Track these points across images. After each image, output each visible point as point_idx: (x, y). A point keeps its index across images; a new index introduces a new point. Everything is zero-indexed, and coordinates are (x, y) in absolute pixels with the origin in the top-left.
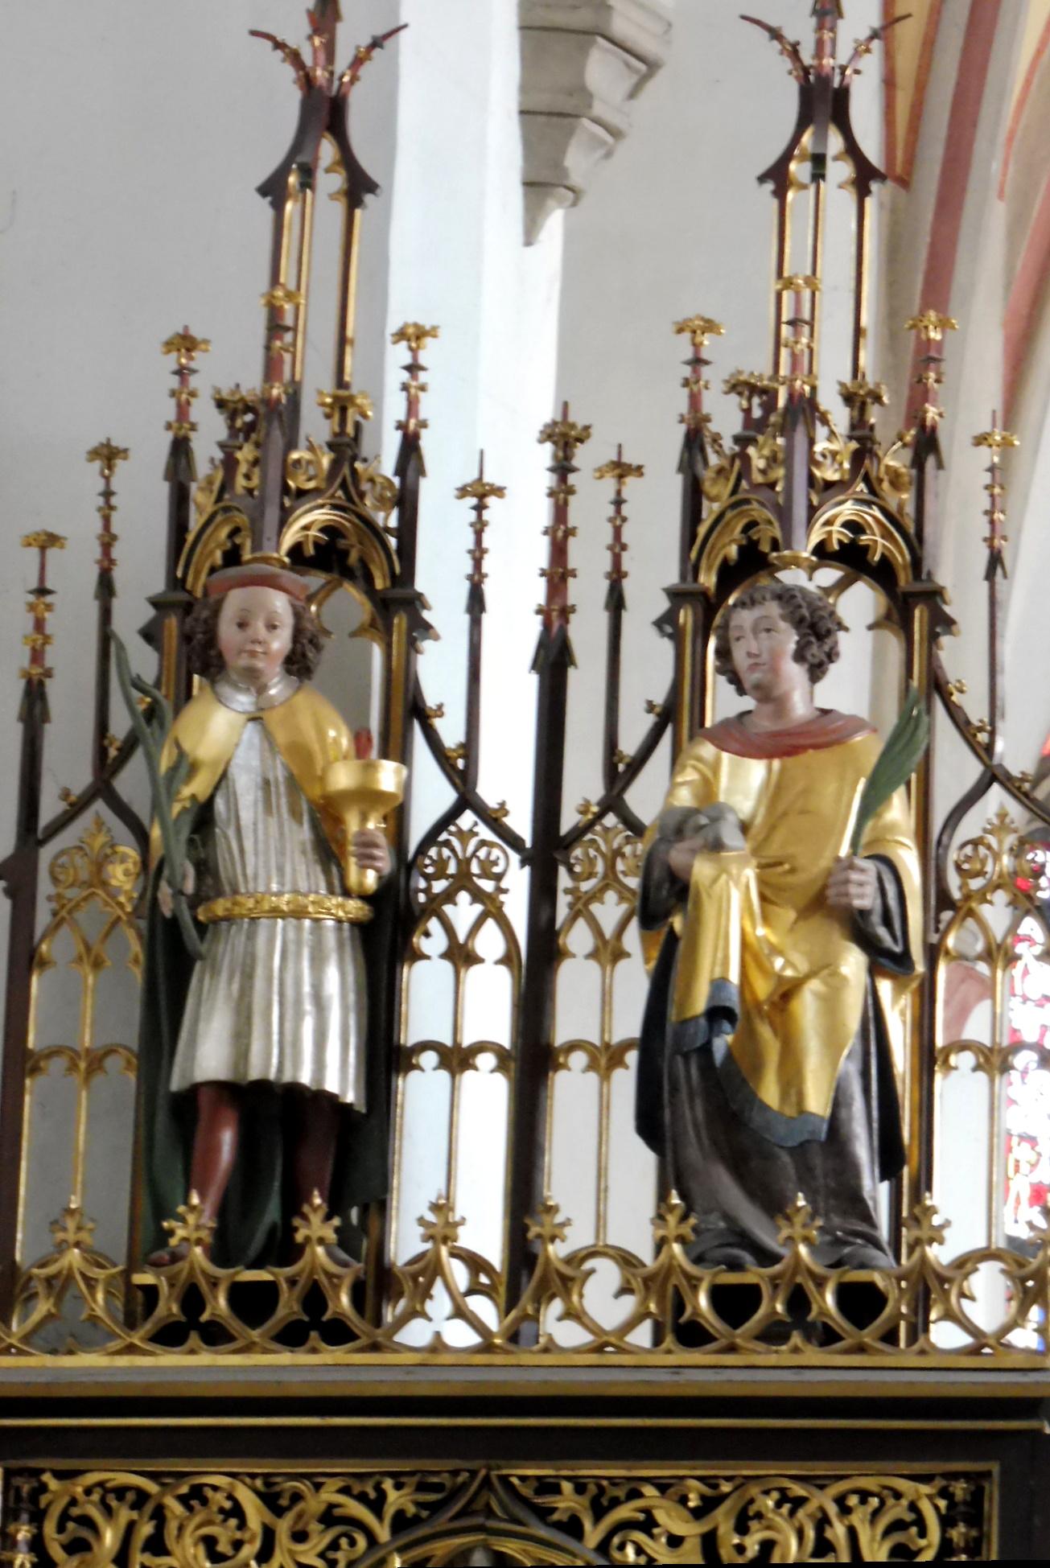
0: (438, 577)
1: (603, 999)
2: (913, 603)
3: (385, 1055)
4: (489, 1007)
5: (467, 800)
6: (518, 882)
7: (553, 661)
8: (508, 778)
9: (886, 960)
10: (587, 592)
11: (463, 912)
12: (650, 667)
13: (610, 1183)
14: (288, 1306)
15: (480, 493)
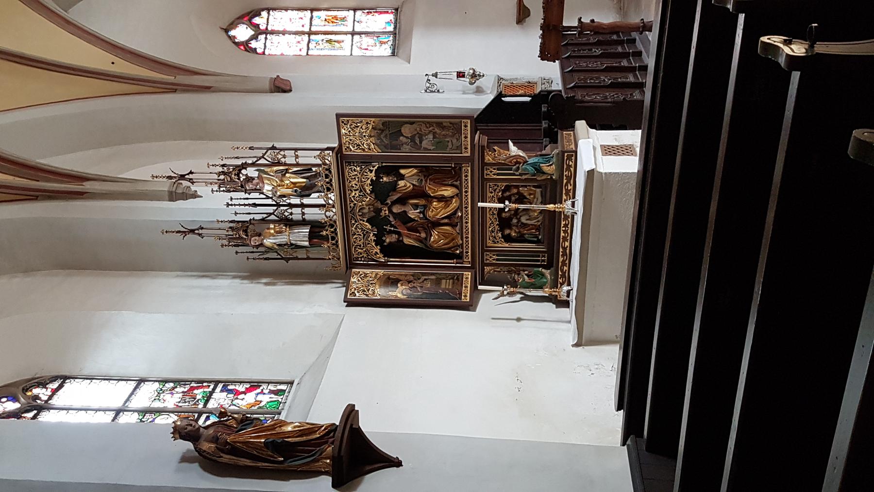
0: (247, 218)
1: (296, 201)
2: (244, 166)
3: (303, 223)
4: (298, 210)
5: (273, 214)
6: (282, 208)
7: (255, 205)
8: (271, 209)
9: (287, 171)
10: (247, 202)
11: (286, 214)
12: (256, 195)
13: (315, 198)
14: (333, 235)
15: (236, 214)
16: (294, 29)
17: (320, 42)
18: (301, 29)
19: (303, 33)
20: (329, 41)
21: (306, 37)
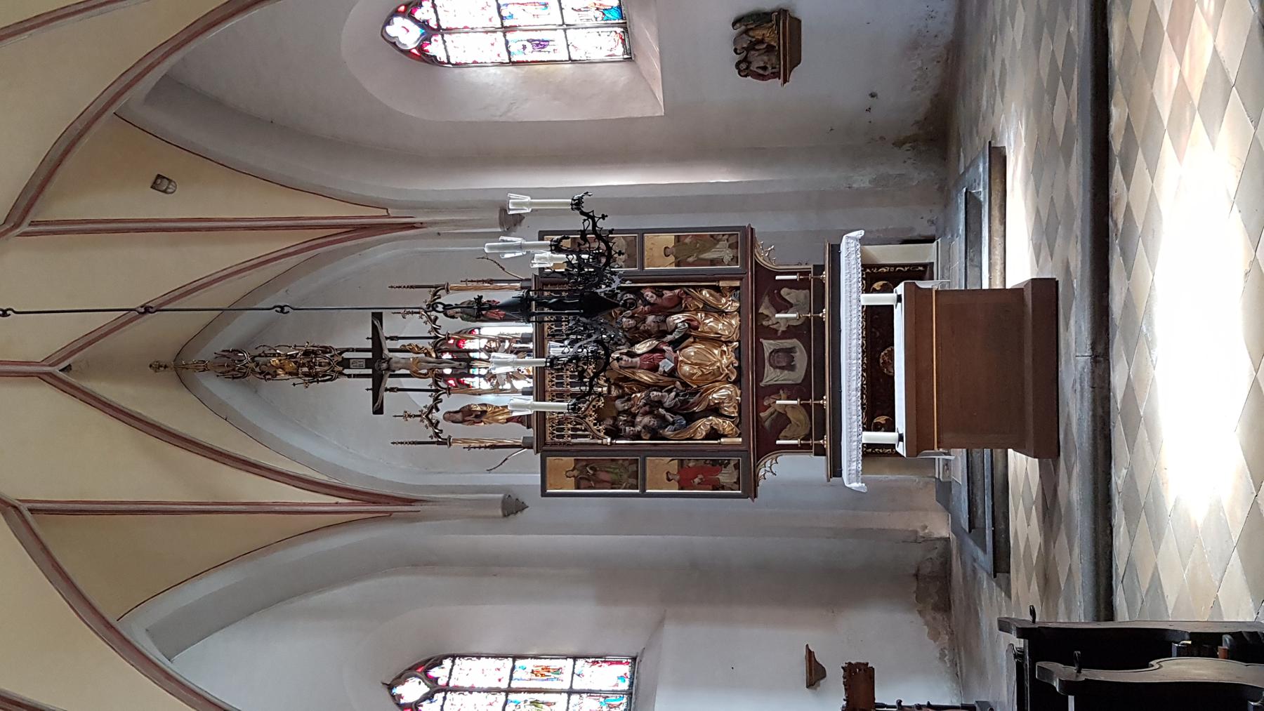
16: (486, 686)
17: (522, 704)
18: (495, 684)
19: (499, 690)
20: (535, 703)
21: (502, 696)
